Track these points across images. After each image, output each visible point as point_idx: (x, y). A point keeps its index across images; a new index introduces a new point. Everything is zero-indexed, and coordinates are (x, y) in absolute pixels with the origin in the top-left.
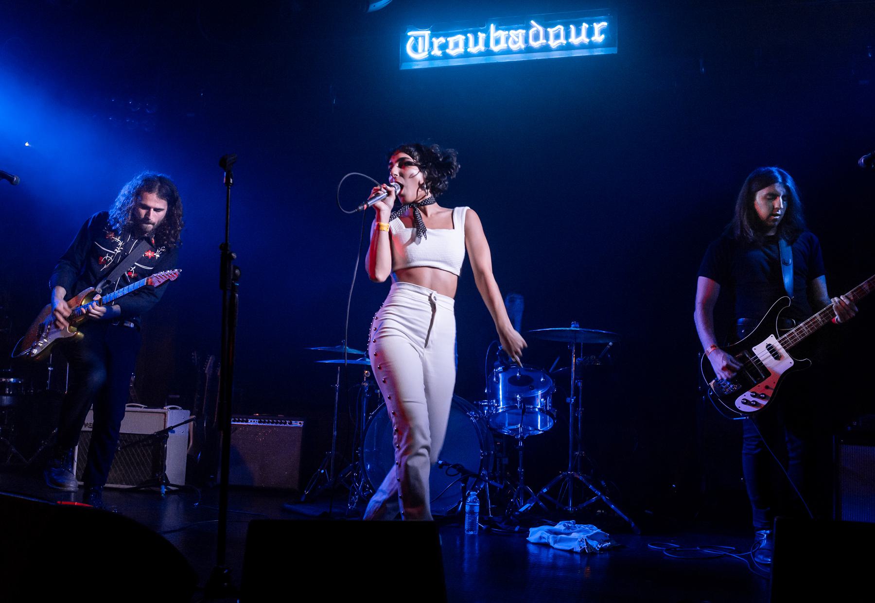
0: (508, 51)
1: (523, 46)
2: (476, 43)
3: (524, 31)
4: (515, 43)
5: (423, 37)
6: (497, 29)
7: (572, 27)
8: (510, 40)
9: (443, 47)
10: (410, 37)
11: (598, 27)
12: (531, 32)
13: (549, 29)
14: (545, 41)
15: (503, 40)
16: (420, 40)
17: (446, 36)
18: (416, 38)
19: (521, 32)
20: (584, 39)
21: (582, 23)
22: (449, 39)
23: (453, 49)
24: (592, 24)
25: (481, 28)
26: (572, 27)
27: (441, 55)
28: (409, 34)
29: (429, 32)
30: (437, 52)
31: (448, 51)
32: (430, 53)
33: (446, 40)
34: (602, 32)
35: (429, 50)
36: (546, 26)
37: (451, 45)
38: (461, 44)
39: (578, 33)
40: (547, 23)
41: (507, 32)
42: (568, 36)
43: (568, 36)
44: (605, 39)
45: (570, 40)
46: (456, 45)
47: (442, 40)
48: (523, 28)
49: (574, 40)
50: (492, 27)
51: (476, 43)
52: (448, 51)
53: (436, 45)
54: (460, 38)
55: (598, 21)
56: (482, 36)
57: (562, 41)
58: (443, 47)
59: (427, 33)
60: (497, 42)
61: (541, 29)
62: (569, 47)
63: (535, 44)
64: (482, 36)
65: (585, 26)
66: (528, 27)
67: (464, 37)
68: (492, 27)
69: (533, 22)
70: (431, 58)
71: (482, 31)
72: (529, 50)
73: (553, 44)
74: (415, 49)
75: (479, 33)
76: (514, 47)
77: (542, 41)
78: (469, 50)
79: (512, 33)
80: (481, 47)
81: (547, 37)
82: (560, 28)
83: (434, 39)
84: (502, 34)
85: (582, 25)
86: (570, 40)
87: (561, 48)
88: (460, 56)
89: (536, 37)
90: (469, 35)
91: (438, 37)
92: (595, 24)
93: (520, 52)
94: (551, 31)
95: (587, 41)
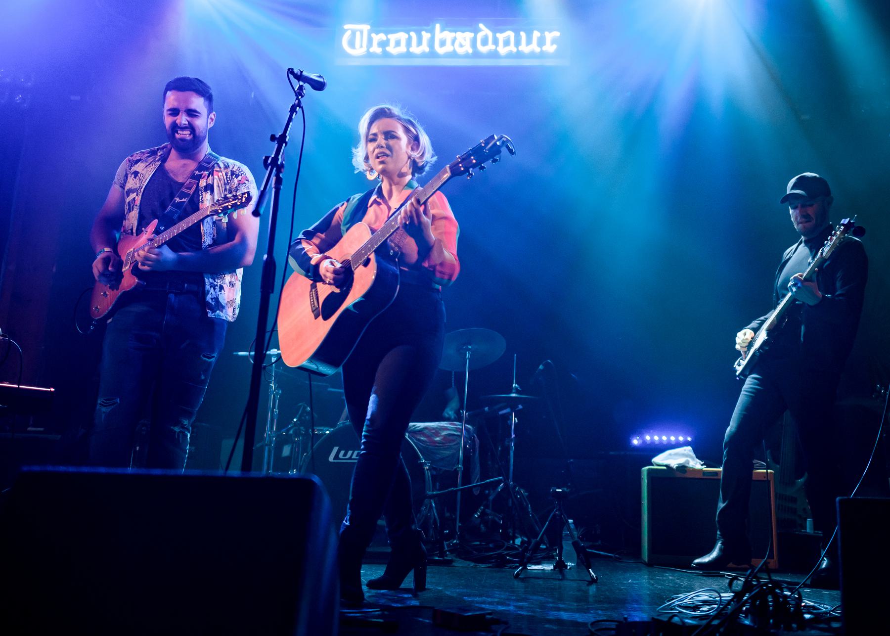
0: (454, 55)
1: (470, 51)
2: (420, 43)
3: (472, 35)
4: (461, 46)
5: (362, 32)
6: (442, 30)
7: (523, 34)
8: (457, 44)
9: (384, 44)
10: (347, 30)
11: (549, 36)
12: (480, 36)
13: (498, 35)
14: (493, 47)
15: (449, 42)
16: (358, 34)
17: (387, 33)
18: (354, 33)
19: (469, 35)
20: (534, 47)
21: (533, 31)
22: (390, 36)
23: (394, 48)
24: (544, 33)
25: (426, 28)
26: (523, 34)
27: (381, 54)
28: (346, 27)
29: (369, 27)
30: (376, 49)
31: (388, 49)
32: (368, 50)
33: (387, 37)
34: (553, 42)
35: (367, 47)
36: (495, 31)
37: (392, 43)
38: (403, 43)
39: (529, 42)
40: (497, 27)
41: (453, 34)
42: (518, 43)
43: (518, 43)
44: (557, 51)
45: (520, 48)
46: (398, 43)
47: (382, 37)
48: (471, 31)
49: (524, 48)
50: (438, 26)
51: (420, 43)
52: (388, 49)
53: (375, 43)
54: (402, 36)
55: (550, 31)
56: (426, 36)
57: (512, 48)
58: (384, 44)
59: (366, 28)
60: (443, 43)
61: (490, 34)
62: (519, 55)
63: (483, 49)
64: (426, 36)
65: (536, 34)
66: (476, 31)
67: (406, 36)
68: (438, 26)
69: (481, 26)
70: (369, 55)
71: (427, 31)
72: (476, 54)
73: (503, 50)
74: (352, 44)
75: (423, 33)
76: (461, 51)
77: (491, 47)
78: (411, 50)
79: (459, 35)
80: (425, 48)
81: (496, 42)
82: (510, 34)
83: (373, 35)
84: (448, 35)
85: (532, 33)
86: (520, 48)
87: (510, 55)
88: (401, 56)
89: (485, 42)
90: (413, 34)
91: (377, 33)
92: (547, 33)
93: (467, 56)
94: (501, 37)
95: (538, 50)
